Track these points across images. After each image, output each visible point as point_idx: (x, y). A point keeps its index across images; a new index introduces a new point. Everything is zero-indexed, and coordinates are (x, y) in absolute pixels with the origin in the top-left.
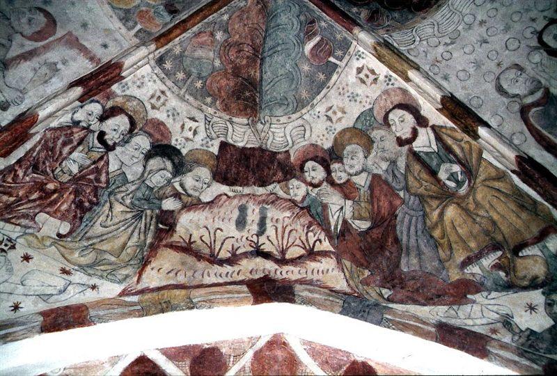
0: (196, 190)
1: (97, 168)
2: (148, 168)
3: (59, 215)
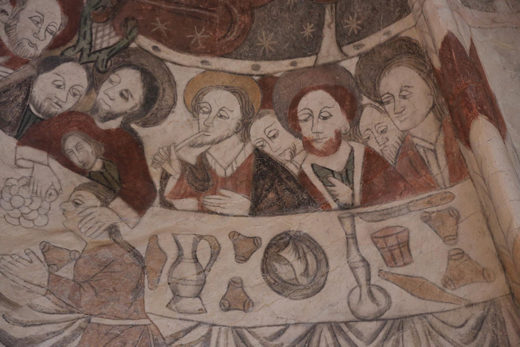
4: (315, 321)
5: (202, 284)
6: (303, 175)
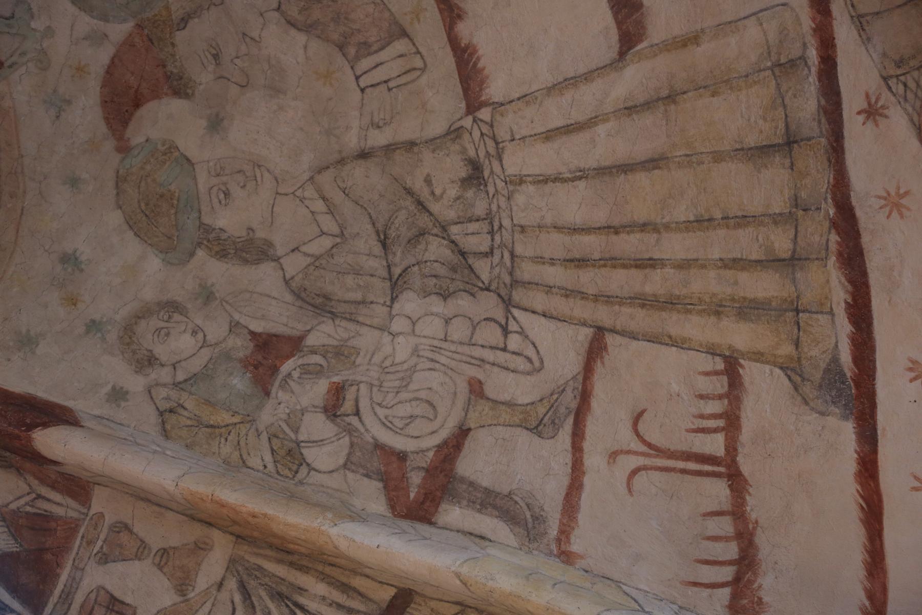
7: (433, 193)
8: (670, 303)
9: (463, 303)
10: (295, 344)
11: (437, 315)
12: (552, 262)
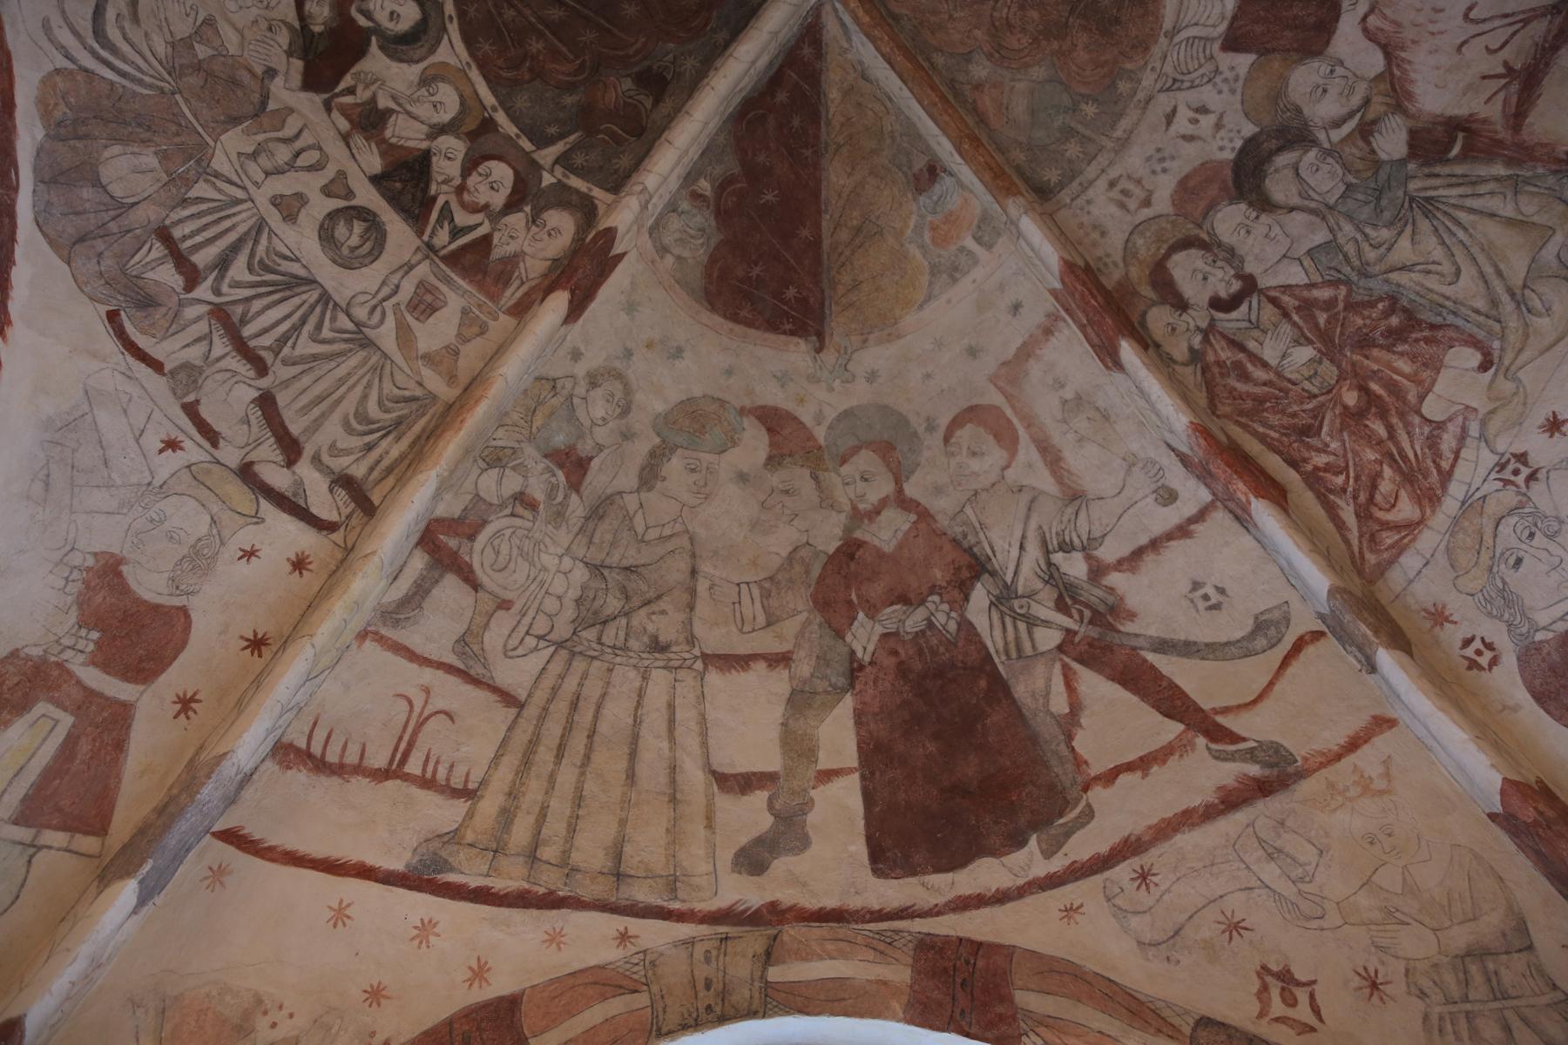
0: (1352, 89)
1: (1298, 309)
2: (1296, 201)
3: (1425, 375)
4: (319, 279)
5: (279, 171)
6: (434, 199)
7: (654, 613)
8: (527, 761)
9: (569, 613)
10: (575, 486)
11: (566, 592)
12: (581, 685)
